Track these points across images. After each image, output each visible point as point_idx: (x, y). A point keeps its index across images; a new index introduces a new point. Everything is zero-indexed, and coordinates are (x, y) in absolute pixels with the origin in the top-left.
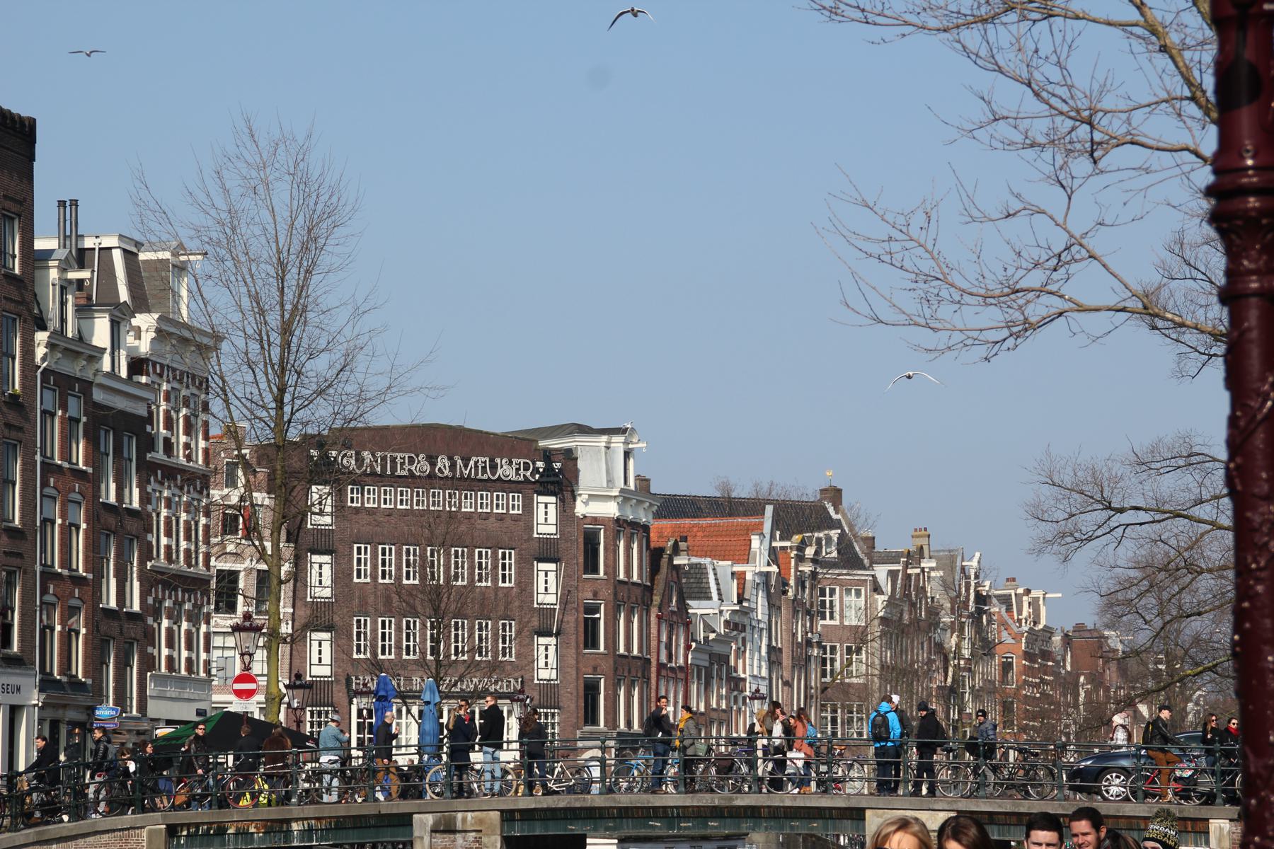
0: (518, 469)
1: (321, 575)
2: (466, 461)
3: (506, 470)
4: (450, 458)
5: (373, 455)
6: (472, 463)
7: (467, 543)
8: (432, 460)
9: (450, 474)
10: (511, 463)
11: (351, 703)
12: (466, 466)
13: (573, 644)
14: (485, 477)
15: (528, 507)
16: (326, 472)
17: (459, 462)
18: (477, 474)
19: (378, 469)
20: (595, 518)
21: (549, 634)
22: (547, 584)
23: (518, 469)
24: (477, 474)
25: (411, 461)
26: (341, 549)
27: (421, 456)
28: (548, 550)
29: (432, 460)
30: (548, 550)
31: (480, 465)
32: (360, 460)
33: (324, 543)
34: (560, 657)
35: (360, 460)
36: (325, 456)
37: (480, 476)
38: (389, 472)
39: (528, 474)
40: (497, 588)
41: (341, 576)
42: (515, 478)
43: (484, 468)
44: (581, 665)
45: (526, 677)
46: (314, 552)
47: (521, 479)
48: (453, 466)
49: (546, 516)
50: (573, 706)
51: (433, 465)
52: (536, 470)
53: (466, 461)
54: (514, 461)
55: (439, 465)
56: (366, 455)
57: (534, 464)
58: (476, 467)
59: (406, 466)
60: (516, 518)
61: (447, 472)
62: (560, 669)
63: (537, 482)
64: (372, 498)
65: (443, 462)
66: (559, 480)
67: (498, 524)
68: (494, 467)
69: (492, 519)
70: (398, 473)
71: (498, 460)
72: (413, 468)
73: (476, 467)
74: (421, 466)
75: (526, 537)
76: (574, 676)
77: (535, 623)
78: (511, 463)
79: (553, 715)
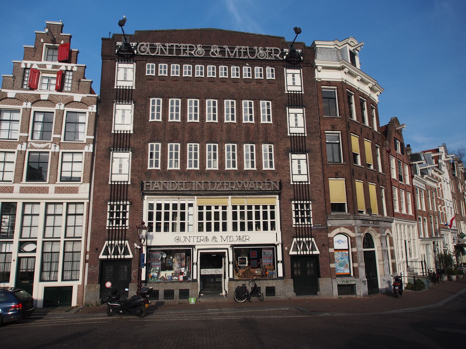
0: (270, 53)
1: (123, 118)
2: (232, 49)
3: (261, 53)
5: (163, 46)
6: (236, 50)
9: (220, 56)
10: (265, 50)
11: (142, 199)
12: (232, 52)
13: (319, 158)
15: (280, 77)
16: (127, 55)
17: (227, 49)
18: (240, 55)
22: (296, 121)
24: (240, 55)
25: (191, 48)
28: (295, 101)
30: (295, 101)
32: (153, 49)
34: (311, 168)
35: (153, 49)
36: (127, 45)
39: (278, 55)
41: (140, 117)
43: (245, 53)
44: (326, 172)
45: (284, 180)
48: (222, 52)
49: (293, 81)
51: (207, 51)
52: (283, 54)
53: (232, 49)
54: (267, 48)
55: (212, 50)
56: (158, 45)
57: (282, 50)
58: (240, 52)
61: (218, 55)
63: (284, 60)
64: (162, 69)
65: (215, 49)
66: (302, 58)
68: (253, 53)
71: (256, 48)
72: (193, 52)
73: (240, 52)
74: (199, 50)
78: (265, 50)
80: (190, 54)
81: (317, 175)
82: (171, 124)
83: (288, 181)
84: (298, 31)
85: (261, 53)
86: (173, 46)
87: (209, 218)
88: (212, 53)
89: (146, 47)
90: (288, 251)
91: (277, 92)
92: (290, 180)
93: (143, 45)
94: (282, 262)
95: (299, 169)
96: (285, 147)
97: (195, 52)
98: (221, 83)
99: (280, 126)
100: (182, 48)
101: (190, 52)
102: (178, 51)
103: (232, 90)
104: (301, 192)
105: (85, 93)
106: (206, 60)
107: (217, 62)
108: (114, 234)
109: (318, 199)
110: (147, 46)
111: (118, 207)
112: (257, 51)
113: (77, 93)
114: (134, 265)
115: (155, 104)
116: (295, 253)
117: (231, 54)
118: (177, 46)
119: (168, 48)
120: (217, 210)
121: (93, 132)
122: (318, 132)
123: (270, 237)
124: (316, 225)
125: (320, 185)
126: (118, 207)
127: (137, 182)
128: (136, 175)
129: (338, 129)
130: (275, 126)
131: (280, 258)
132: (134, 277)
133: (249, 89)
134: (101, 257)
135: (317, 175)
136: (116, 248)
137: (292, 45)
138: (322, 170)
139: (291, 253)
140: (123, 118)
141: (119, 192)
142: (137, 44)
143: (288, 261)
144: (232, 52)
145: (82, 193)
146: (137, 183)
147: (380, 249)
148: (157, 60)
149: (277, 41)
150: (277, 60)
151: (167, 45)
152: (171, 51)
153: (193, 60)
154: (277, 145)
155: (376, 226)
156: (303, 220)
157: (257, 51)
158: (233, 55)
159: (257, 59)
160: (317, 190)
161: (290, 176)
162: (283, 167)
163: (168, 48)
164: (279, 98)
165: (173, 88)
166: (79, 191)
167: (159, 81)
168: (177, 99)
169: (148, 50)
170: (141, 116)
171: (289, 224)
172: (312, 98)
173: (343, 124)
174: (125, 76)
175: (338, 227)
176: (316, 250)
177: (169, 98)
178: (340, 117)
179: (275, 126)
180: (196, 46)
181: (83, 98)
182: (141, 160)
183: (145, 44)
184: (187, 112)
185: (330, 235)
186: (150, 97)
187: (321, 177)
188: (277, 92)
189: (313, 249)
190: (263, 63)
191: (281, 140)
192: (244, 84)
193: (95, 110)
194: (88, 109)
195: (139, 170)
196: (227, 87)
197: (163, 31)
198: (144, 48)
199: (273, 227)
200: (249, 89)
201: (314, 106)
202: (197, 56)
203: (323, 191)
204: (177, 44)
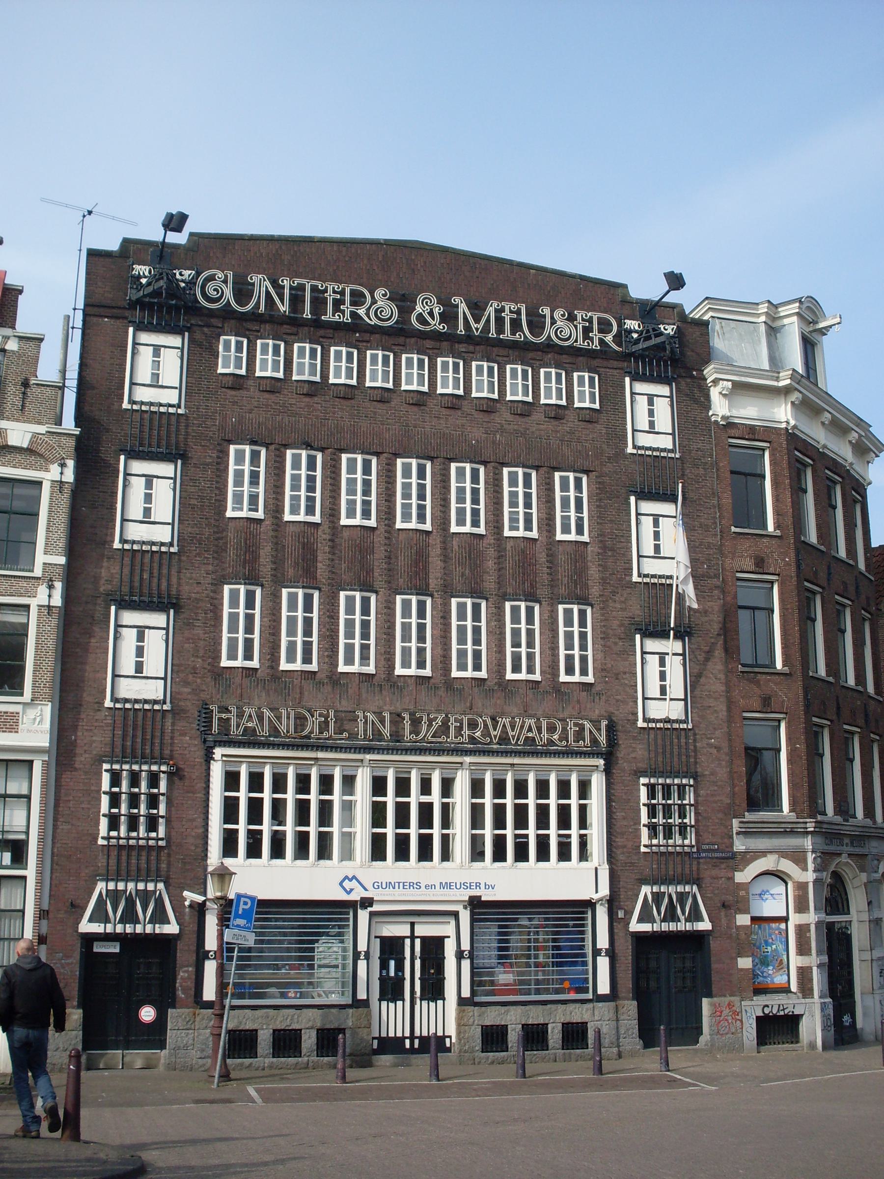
2: (477, 309)
3: (560, 327)
4: (444, 302)
6: (491, 310)
7: (487, 454)
8: (404, 302)
9: (442, 328)
10: (571, 318)
11: (209, 757)
12: (477, 321)
14: (519, 337)
17: (463, 308)
18: (500, 329)
19: (284, 308)
20: (752, 428)
21: (663, 634)
23: (587, 331)
24: (500, 329)
25: (357, 299)
26: (196, 452)
27: (379, 293)
28: (655, 479)
29: (404, 302)
31: (507, 317)
32: (243, 292)
33: (159, 436)
34: (694, 681)
35: (243, 292)
37: (507, 335)
38: (307, 314)
39: (609, 338)
40: (552, 544)
41: (200, 503)
42: (581, 343)
43: (516, 325)
45: (620, 715)
46: (135, 454)
47: (596, 345)
48: (449, 316)
49: (651, 417)
50: (722, 773)
51: (405, 309)
52: (623, 335)
53: (477, 309)
54: (579, 314)
55: (419, 309)
56: (260, 283)
57: (620, 325)
58: (500, 321)
59: (347, 308)
60: (589, 417)
61: (435, 324)
65: (427, 307)
67: (551, 425)
68: (536, 325)
69: (538, 416)
70: (329, 316)
71: (547, 311)
72: (361, 312)
73: (500, 321)
74: (380, 308)
75: (610, 452)
76: (723, 714)
77: (636, 609)
78: (571, 318)
79: (681, 788)
80: (354, 315)
81: (712, 702)
82: (297, 529)
83: (631, 717)
84: (676, 281)
86: (302, 288)
87: (402, 819)
88: (420, 317)
89: (224, 286)
90: (626, 922)
91: (605, 446)
92: (635, 714)
93: (212, 278)
94: (612, 953)
95: (662, 683)
96: (625, 614)
97: (368, 310)
98: (448, 412)
99: (612, 550)
100: (330, 297)
101: (353, 308)
102: (319, 302)
103: (476, 434)
104: (671, 751)
105: (39, 423)
106: (399, 337)
107: (434, 343)
108: (126, 861)
109: (712, 774)
110: (225, 282)
111: (135, 779)
112: (548, 320)
113: (18, 420)
114: (184, 955)
116: (646, 927)
117: (474, 325)
118: (314, 289)
119: (287, 291)
120: (425, 799)
121: (62, 544)
122: (716, 576)
123: (579, 879)
124: (705, 847)
125: (718, 733)
126: (135, 779)
127: (189, 704)
128: (186, 683)
129: (772, 570)
130: (597, 550)
131: (603, 942)
132: (184, 991)
133: (523, 435)
134: (86, 926)
135: (712, 702)
136: (671, 906)
137: (650, 311)
138: (723, 688)
139: (635, 926)
140: (149, 504)
141: (138, 732)
142: (198, 274)
143: (626, 951)
144: (477, 321)
145: (29, 731)
146: (191, 707)
147: (865, 917)
148: (252, 325)
149: (608, 295)
150: (604, 352)
151: (286, 283)
152: (296, 300)
154: (602, 609)
155: (858, 850)
156: (668, 834)
157: (548, 320)
158: (480, 326)
159: (549, 346)
160: (710, 745)
161: (636, 702)
162: (617, 676)
163: (287, 291)
164: (609, 468)
165: (300, 416)
166: (21, 727)
167: (257, 394)
168: (313, 453)
169: (228, 293)
170: (202, 498)
171: (630, 844)
172: (702, 471)
173: (786, 554)
174: (156, 370)
175: (764, 853)
176: (703, 921)
177: (286, 446)
178: (778, 533)
179: (597, 550)
180: (373, 297)
181: (35, 435)
182: (202, 636)
183: (220, 275)
184: (340, 495)
185: (742, 877)
186: (230, 442)
187: (722, 707)
188: (605, 446)
189: (695, 916)
190: (569, 357)
191: (614, 593)
192: (510, 417)
193: (69, 476)
194: (47, 470)
195: (194, 668)
196: (459, 422)
197: (271, 239)
198: (220, 287)
199: (584, 855)
200: (523, 435)
201: (706, 497)
202: (374, 321)
203: (726, 750)
204: (314, 282)
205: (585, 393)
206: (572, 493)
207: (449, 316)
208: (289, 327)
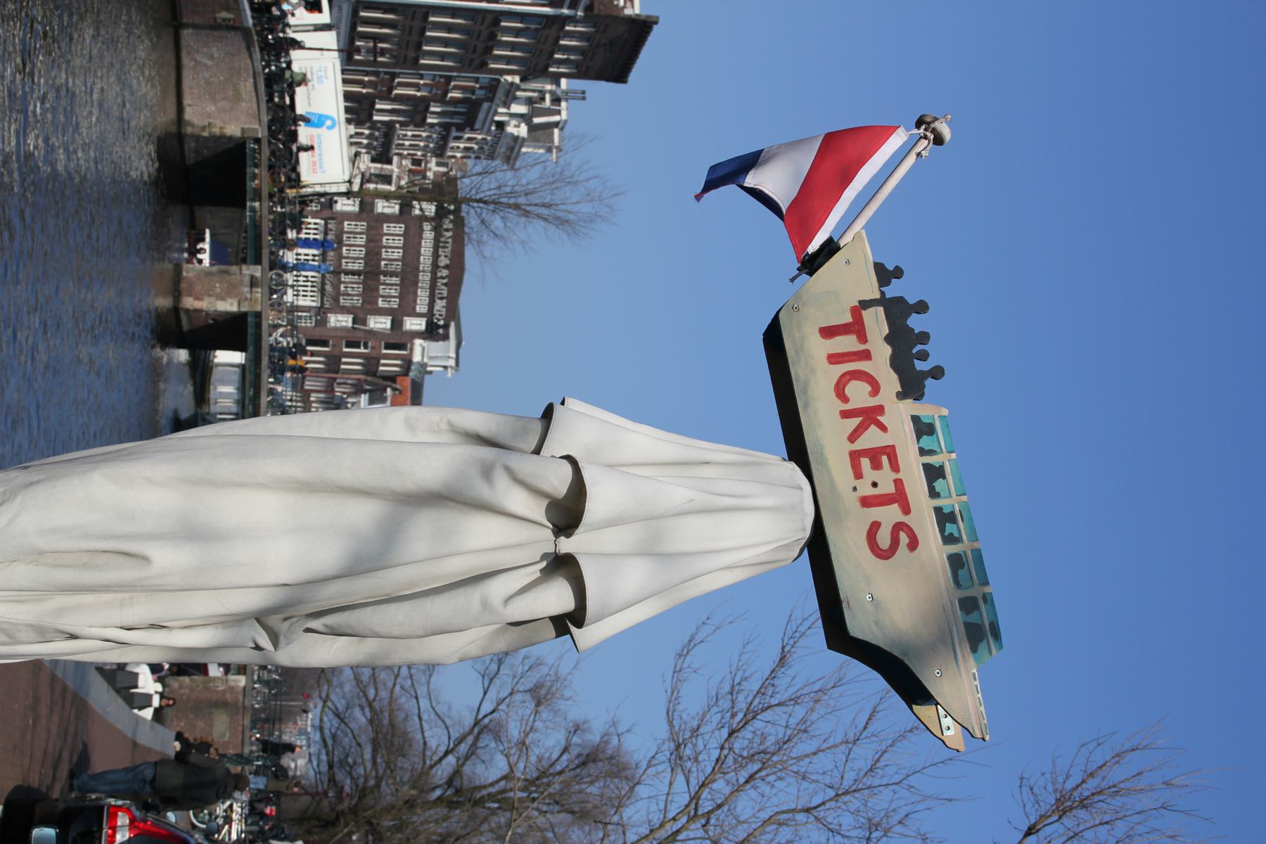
2: (445, 284)
15: (420, 315)
22: (380, 323)
28: (397, 324)
29: (446, 267)
30: (397, 324)
32: (447, 230)
48: (442, 278)
49: (414, 324)
53: (445, 284)
56: (450, 234)
60: (414, 308)
61: (439, 274)
62: (336, 329)
65: (445, 273)
66: (433, 332)
68: (441, 299)
74: (443, 261)
85: (440, 305)
115: (399, 229)
153: (436, 256)
190: (431, 305)
198: (447, 224)
205: (422, 307)
206: (395, 304)
207: (442, 278)
208: (437, 242)
